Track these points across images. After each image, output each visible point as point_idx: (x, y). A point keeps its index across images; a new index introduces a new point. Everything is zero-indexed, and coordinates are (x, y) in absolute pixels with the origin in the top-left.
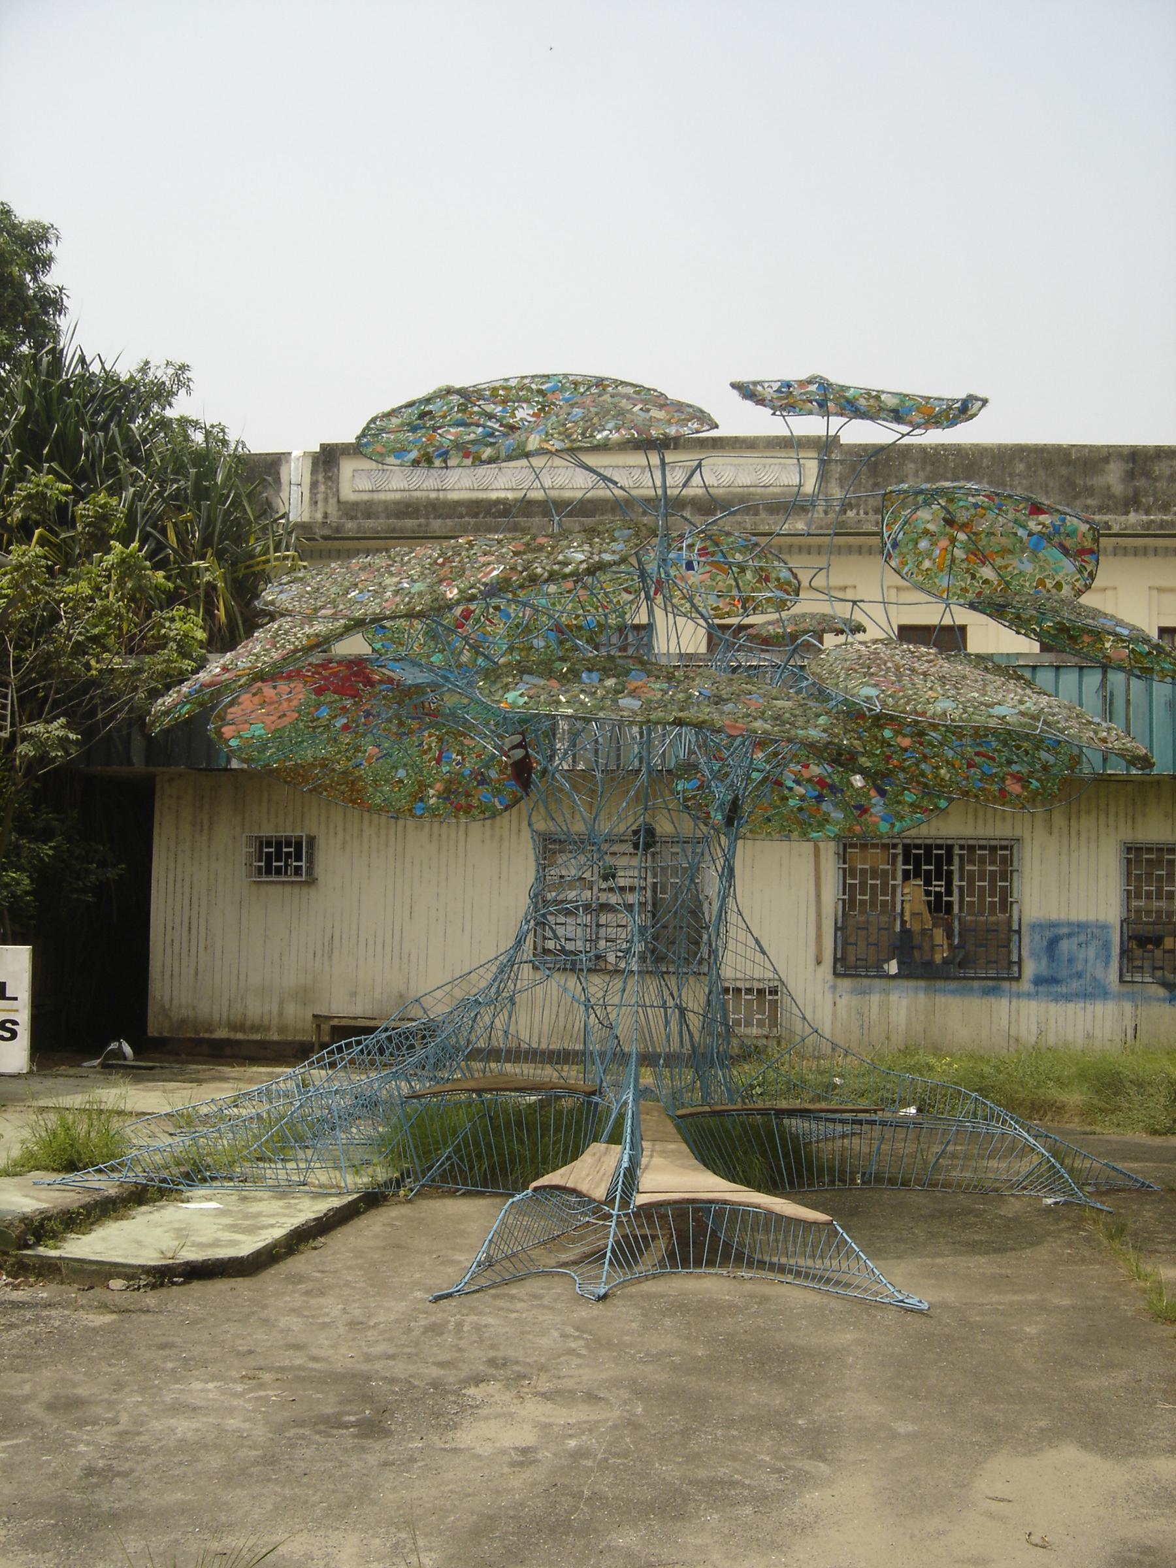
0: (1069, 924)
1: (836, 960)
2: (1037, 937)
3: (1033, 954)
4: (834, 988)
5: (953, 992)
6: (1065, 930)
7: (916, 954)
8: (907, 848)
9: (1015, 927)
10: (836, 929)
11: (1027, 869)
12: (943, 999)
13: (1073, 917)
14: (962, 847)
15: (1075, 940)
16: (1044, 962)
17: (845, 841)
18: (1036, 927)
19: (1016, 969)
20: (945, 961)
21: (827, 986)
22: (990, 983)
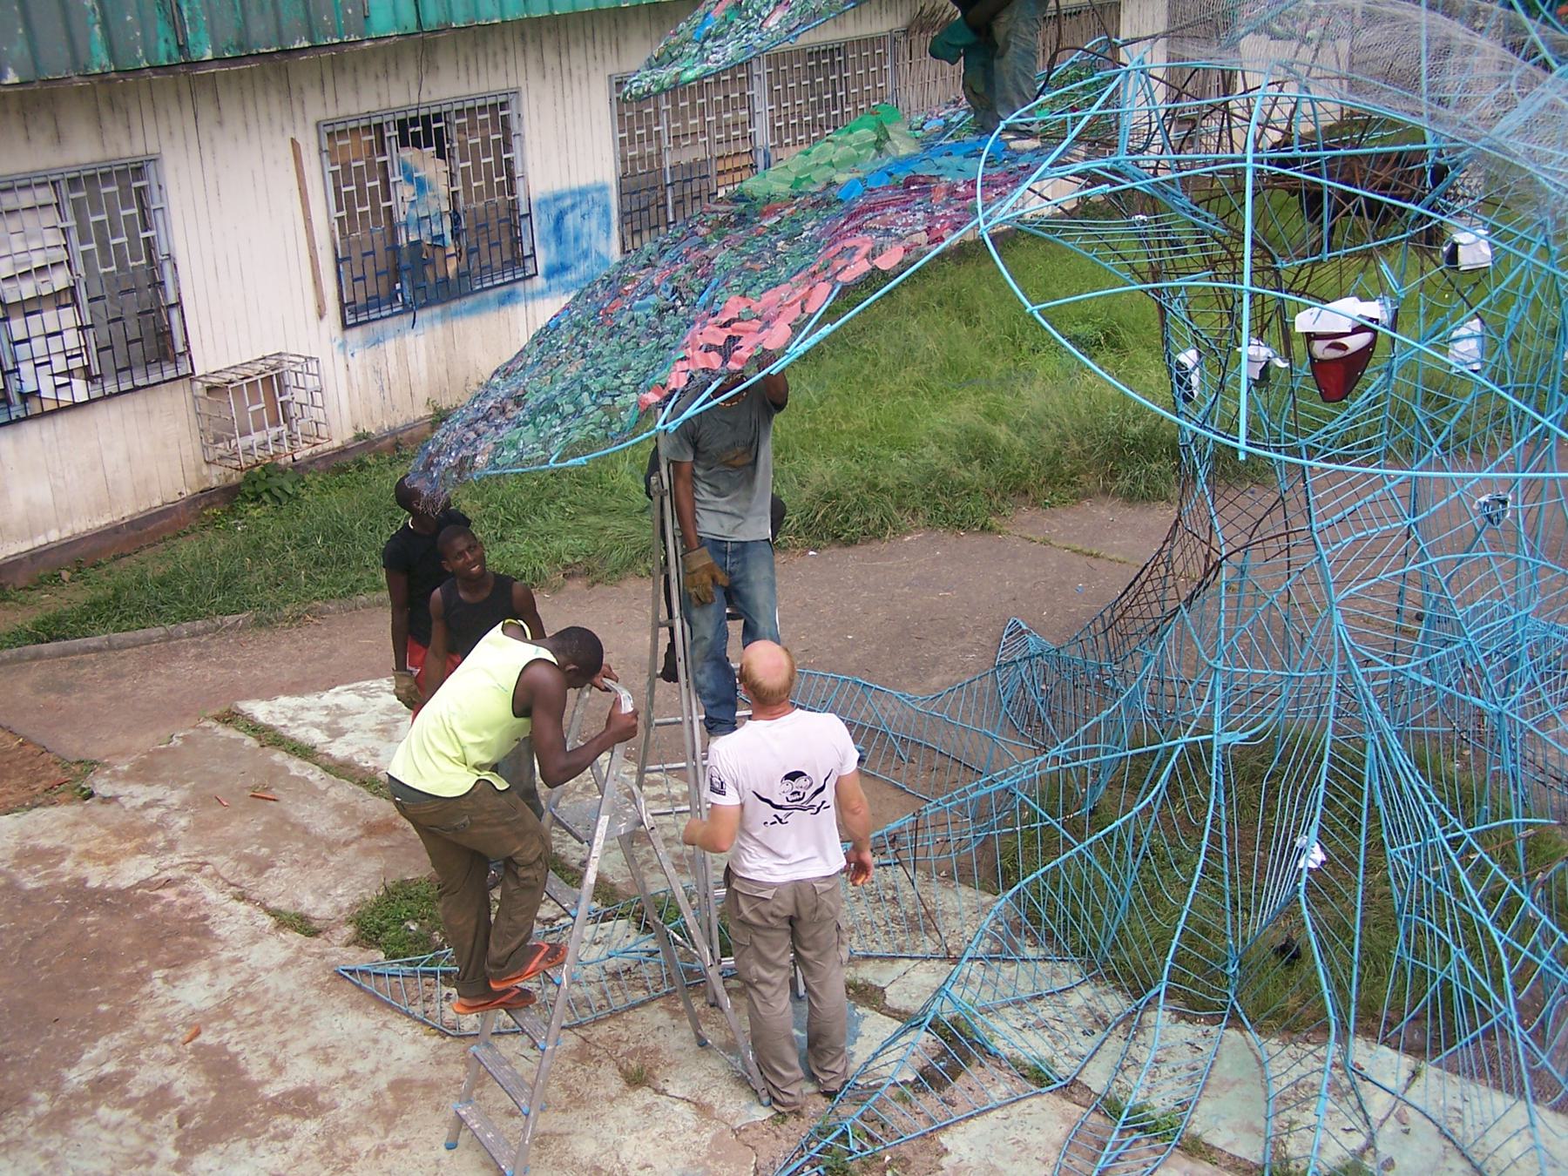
0: (572, 193)
1: (343, 306)
2: (544, 217)
3: (545, 241)
4: (344, 345)
5: (471, 311)
6: (568, 202)
7: (429, 271)
8: (402, 125)
9: (524, 211)
10: (338, 261)
11: (527, 131)
12: (460, 324)
13: (575, 185)
14: (459, 113)
15: (578, 212)
16: (553, 247)
17: (329, 129)
18: (544, 203)
19: (529, 263)
20: (460, 275)
21: (336, 344)
22: (505, 289)
